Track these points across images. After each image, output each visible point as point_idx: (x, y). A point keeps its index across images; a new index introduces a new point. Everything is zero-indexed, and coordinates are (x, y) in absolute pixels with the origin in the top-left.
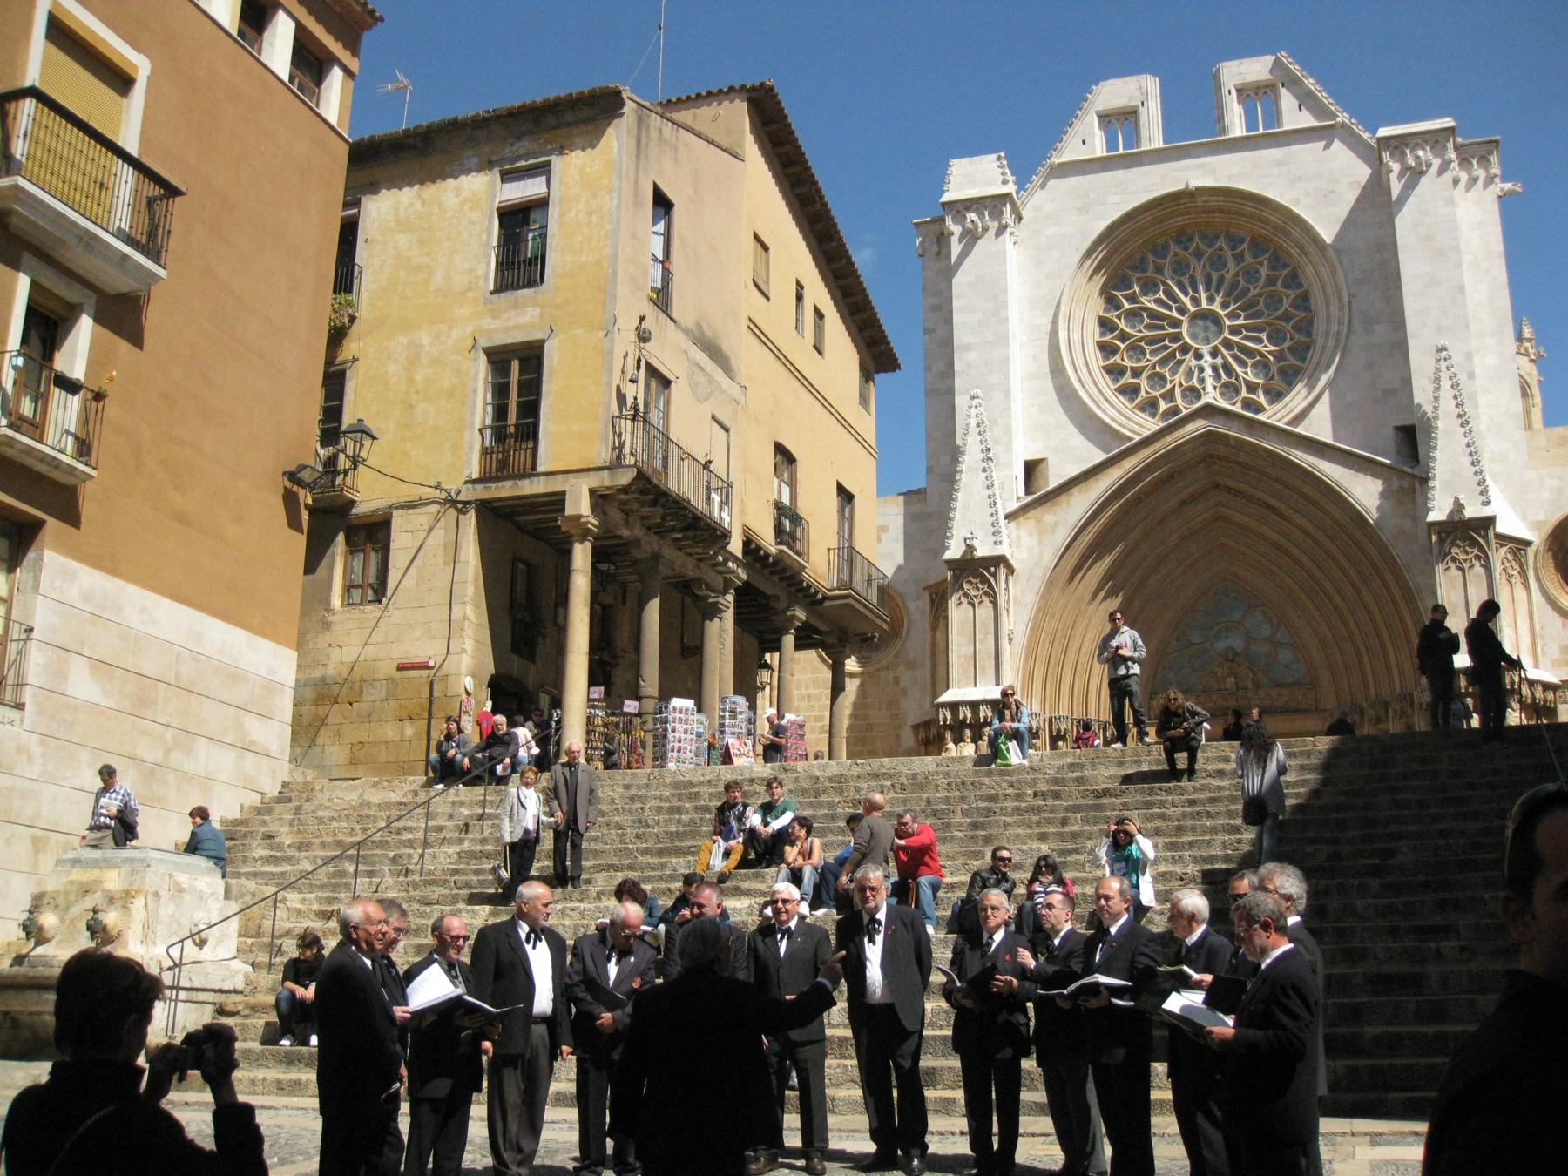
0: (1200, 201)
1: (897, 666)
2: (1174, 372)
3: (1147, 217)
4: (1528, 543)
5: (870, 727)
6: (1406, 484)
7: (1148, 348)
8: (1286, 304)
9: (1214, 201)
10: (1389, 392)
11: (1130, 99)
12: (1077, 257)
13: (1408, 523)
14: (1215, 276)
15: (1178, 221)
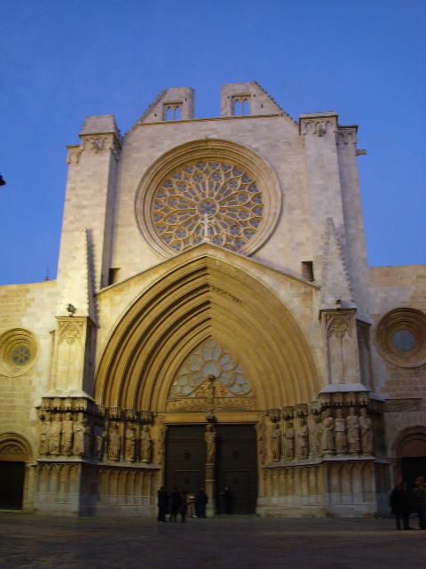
0: (211, 145)
1: (31, 375)
2: (190, 229)
3: (183, 151)
4: (370, 325)
5: (13, 408)
6: (308, 290)
7: (178, 217)
8: (250, 199)
9: (217, 145)
10: (300, 244)
11: (181, 97)
12: (145, 169)
13: (308, 311)
14: (215, 183)
15: (198, 155)
